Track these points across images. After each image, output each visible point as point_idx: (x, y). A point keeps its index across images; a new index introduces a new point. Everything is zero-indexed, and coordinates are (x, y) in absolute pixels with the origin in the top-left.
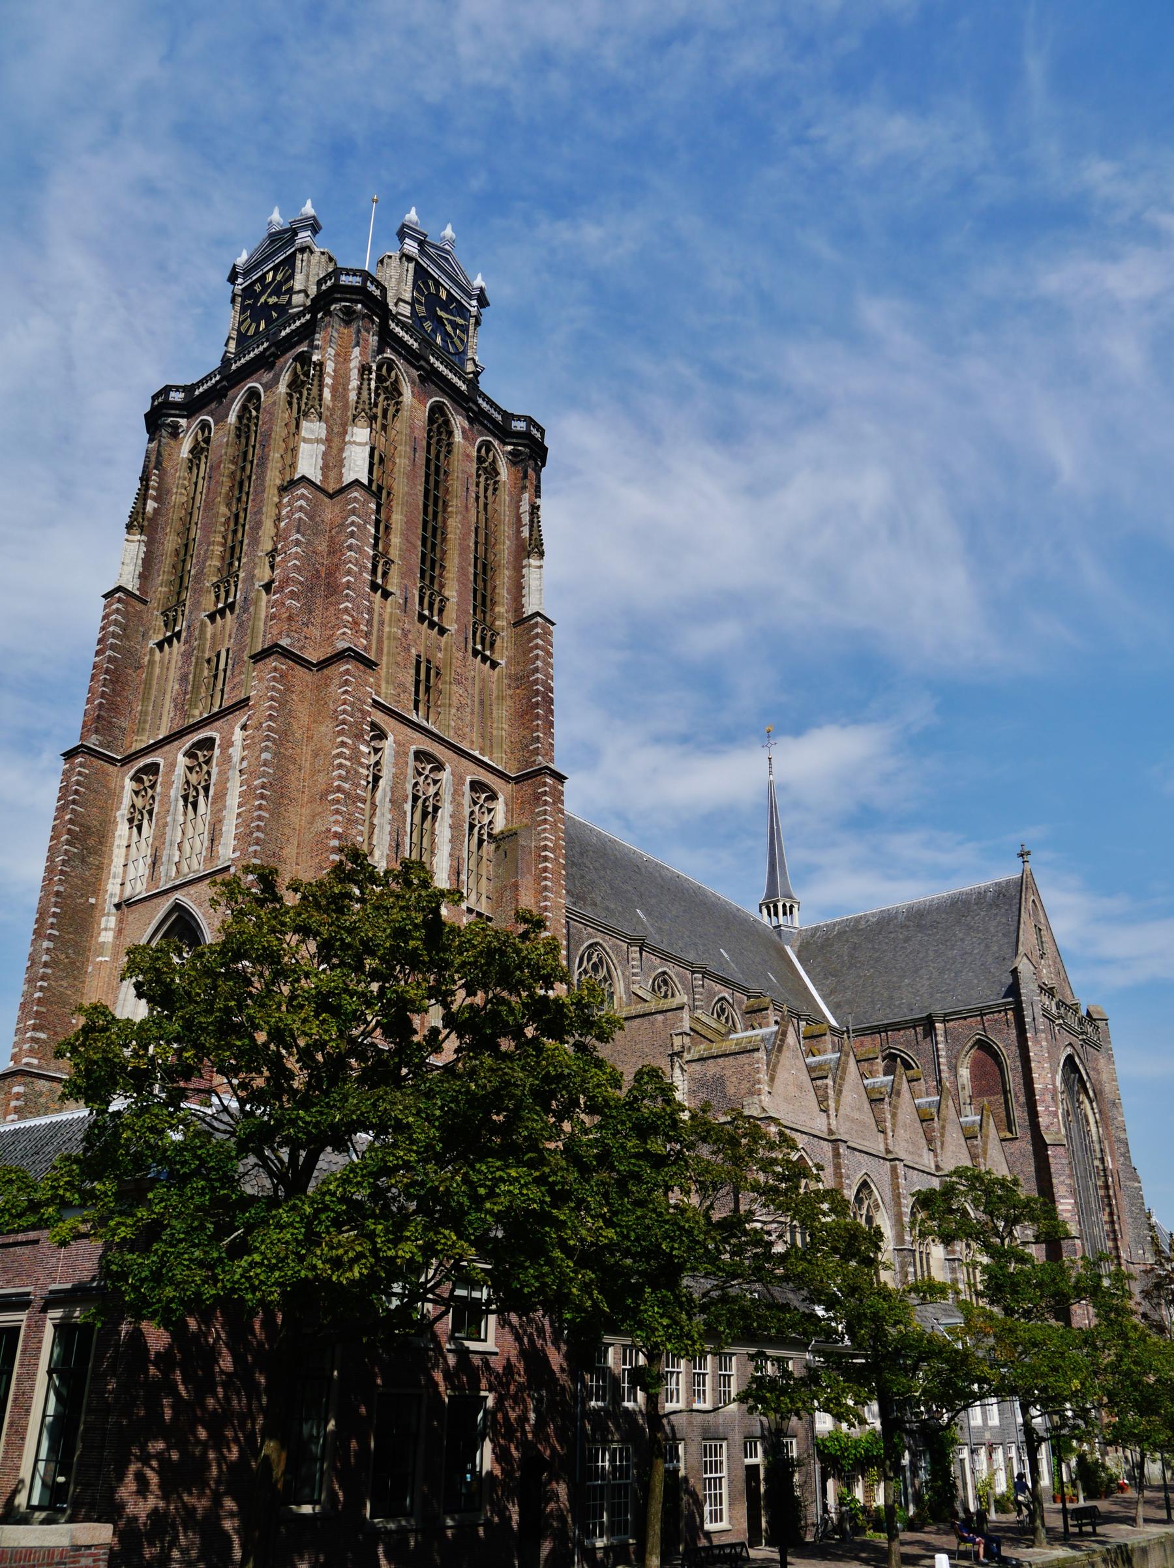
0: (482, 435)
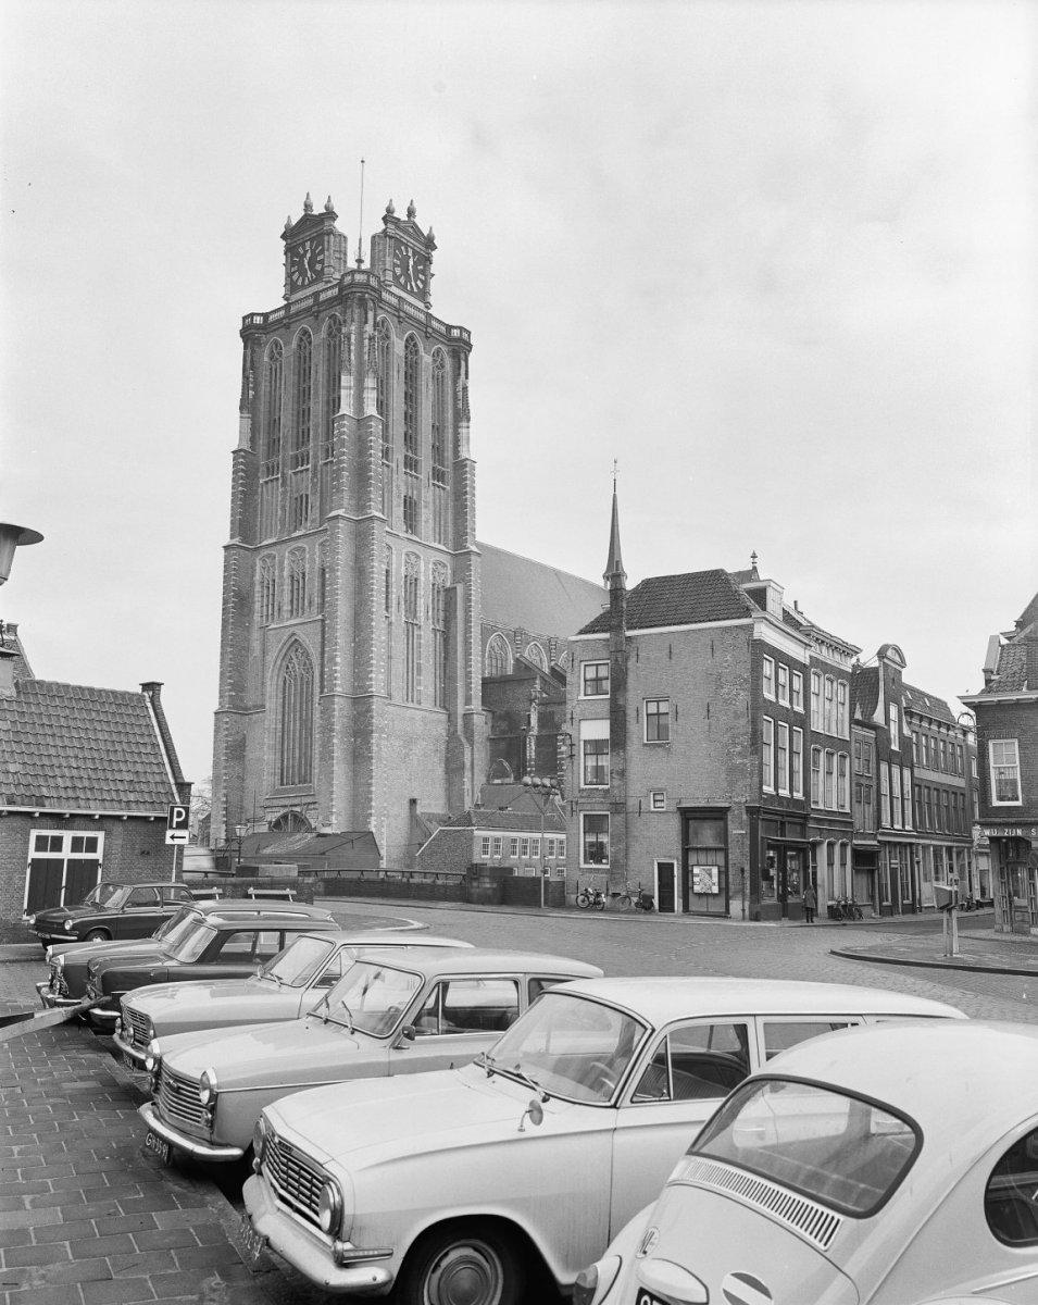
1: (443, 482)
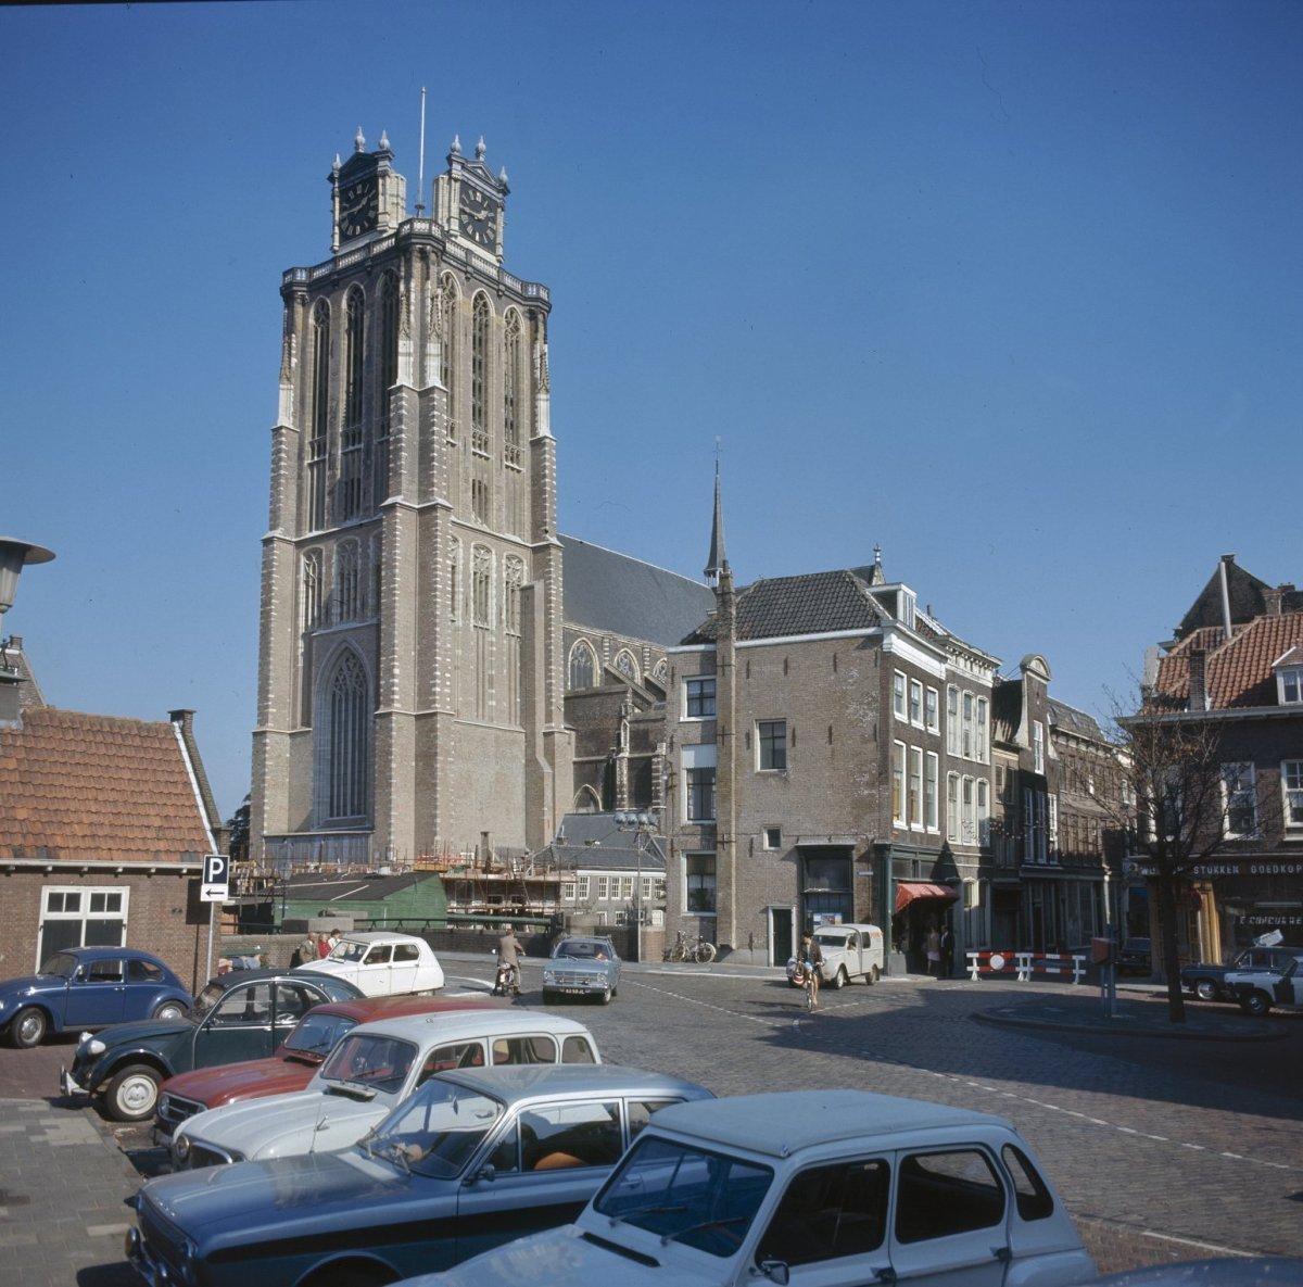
0: (507, 305)
1: (518, 464)
